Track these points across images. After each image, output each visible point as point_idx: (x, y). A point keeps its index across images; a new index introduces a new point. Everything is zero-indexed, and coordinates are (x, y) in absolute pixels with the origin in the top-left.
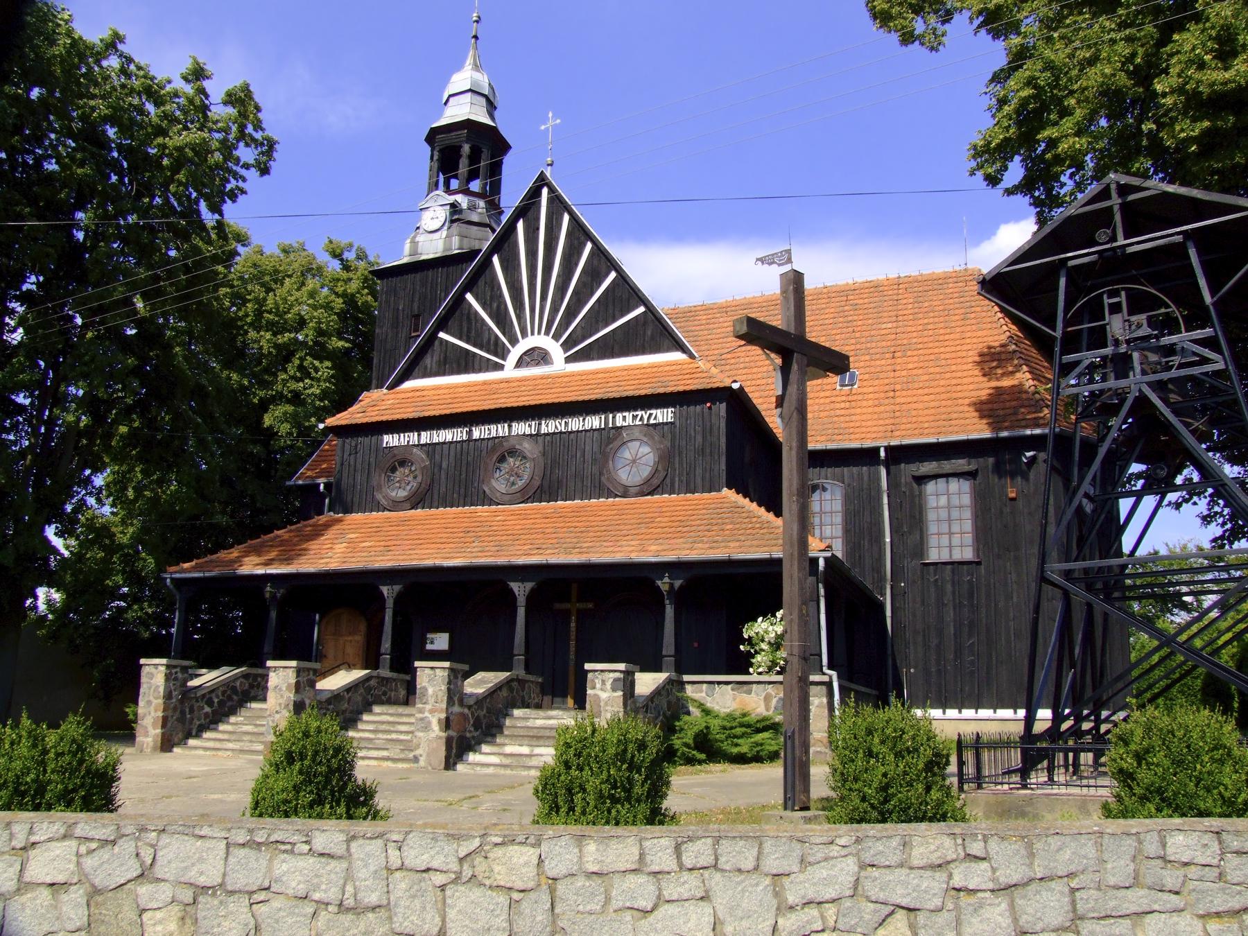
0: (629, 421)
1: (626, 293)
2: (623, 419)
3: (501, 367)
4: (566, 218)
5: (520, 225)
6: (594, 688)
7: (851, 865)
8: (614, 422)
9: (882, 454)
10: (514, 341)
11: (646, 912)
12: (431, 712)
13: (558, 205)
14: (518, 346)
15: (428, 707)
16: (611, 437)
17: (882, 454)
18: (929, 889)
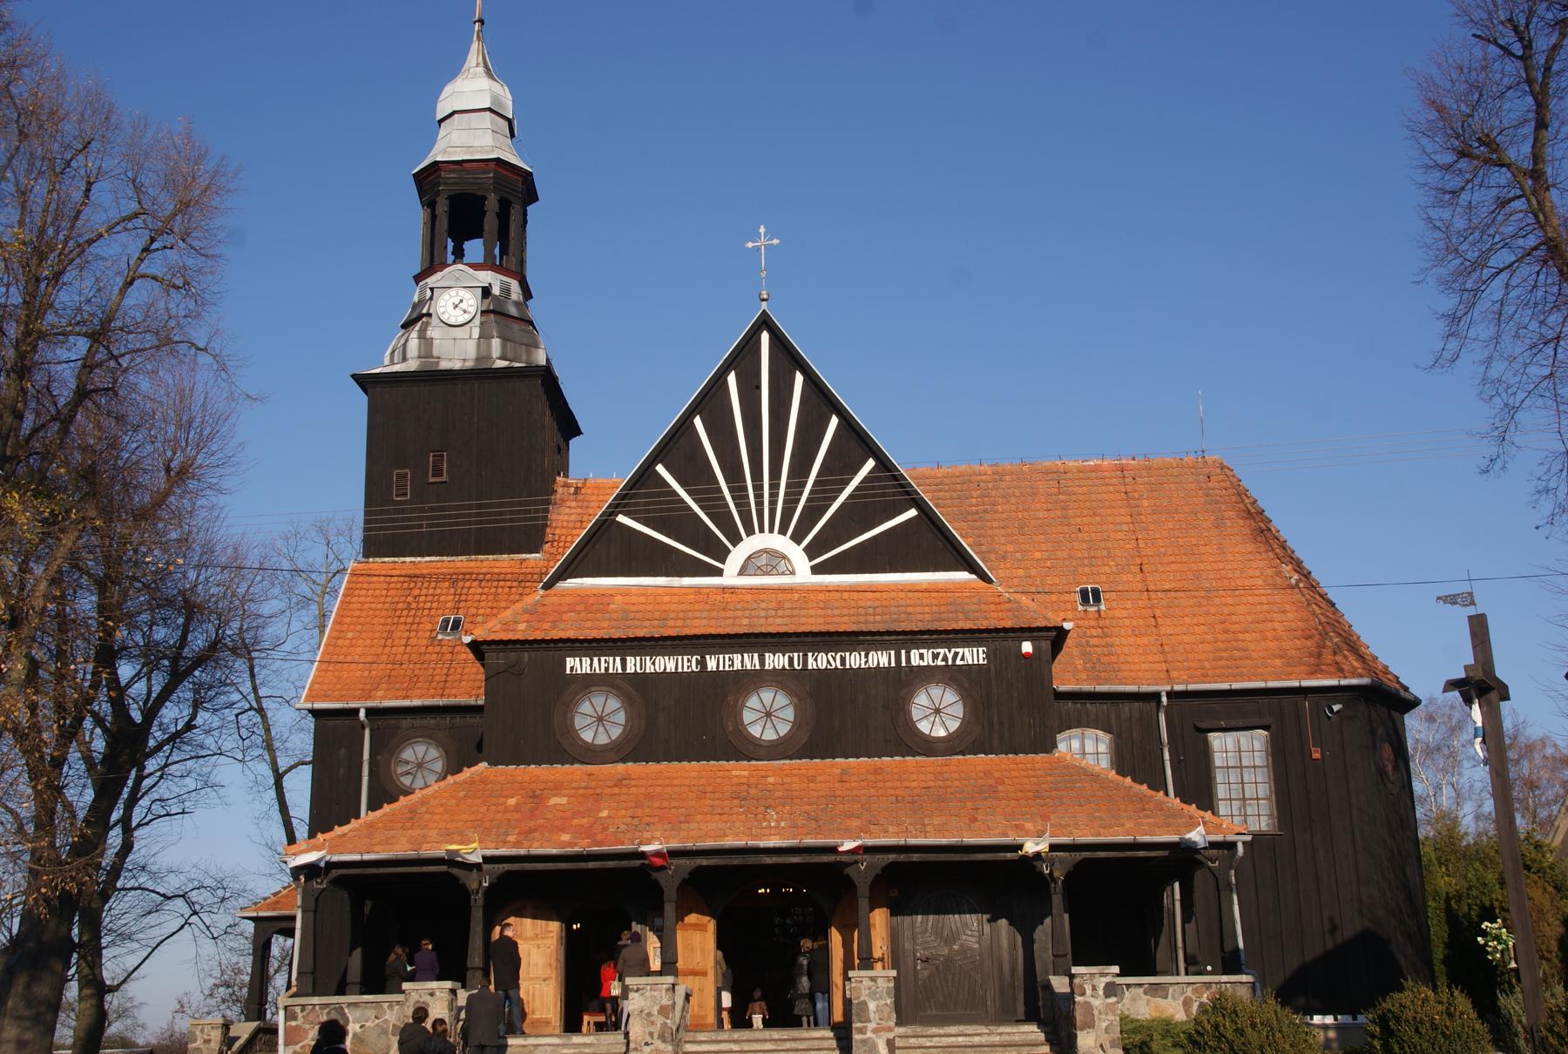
0: (928, 660)
1: (891, 488)
2: (920, 657)
3: (719, 572)
4: (799, 378)
5: (732, 379)
6: (1083, 994)
9: (1164, 699)
10: (736, 539)
12: (875, 1031)
13: (788, 358)
15: (871, 1026)
16: (905, 681)
17: (1164, 699)
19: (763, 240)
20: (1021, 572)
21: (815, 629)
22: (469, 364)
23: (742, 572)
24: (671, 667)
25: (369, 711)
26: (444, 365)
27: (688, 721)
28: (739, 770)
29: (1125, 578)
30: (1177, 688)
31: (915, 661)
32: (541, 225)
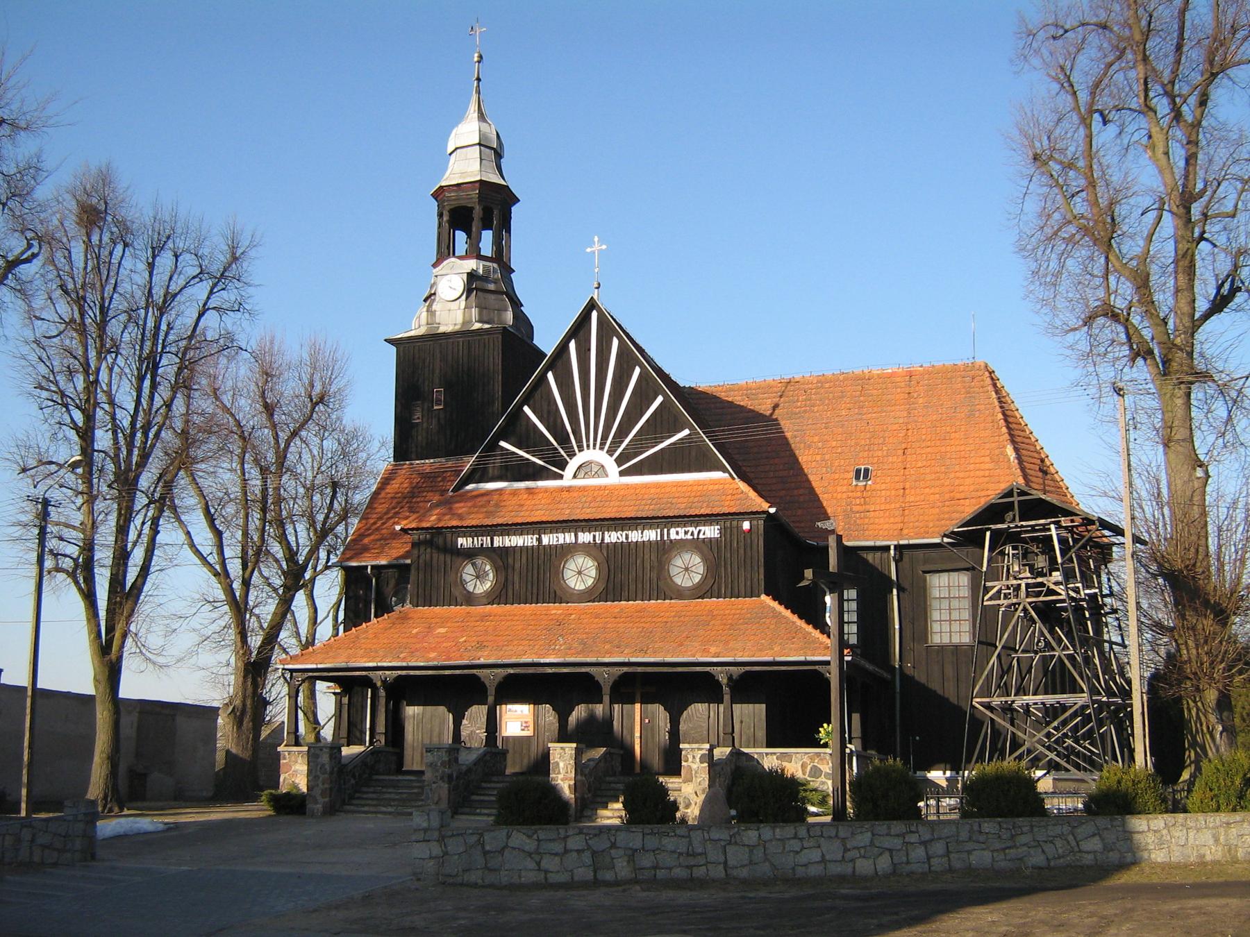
0: (682, 536)
3: (561, 477)
4: (615, 342)
7: (869, 834)
8: (668, 534)
10: (572, 455)
11: (797, 853)
13: (608, 328)
14: (575, 458)
15: (561, 776)
16: (664, 550)
18: (897, 843)
19: (597, 247)
20: (818, 458)
21: (608, 516)
22: (458, 327)
23: (575, 476)
24: (520, 543)
25: (373, 567)
26: (442, 329)
27: (529, 579)
28: (556, 609)
29: (890, 459)
30: (902, 542)
31: (673, 536)
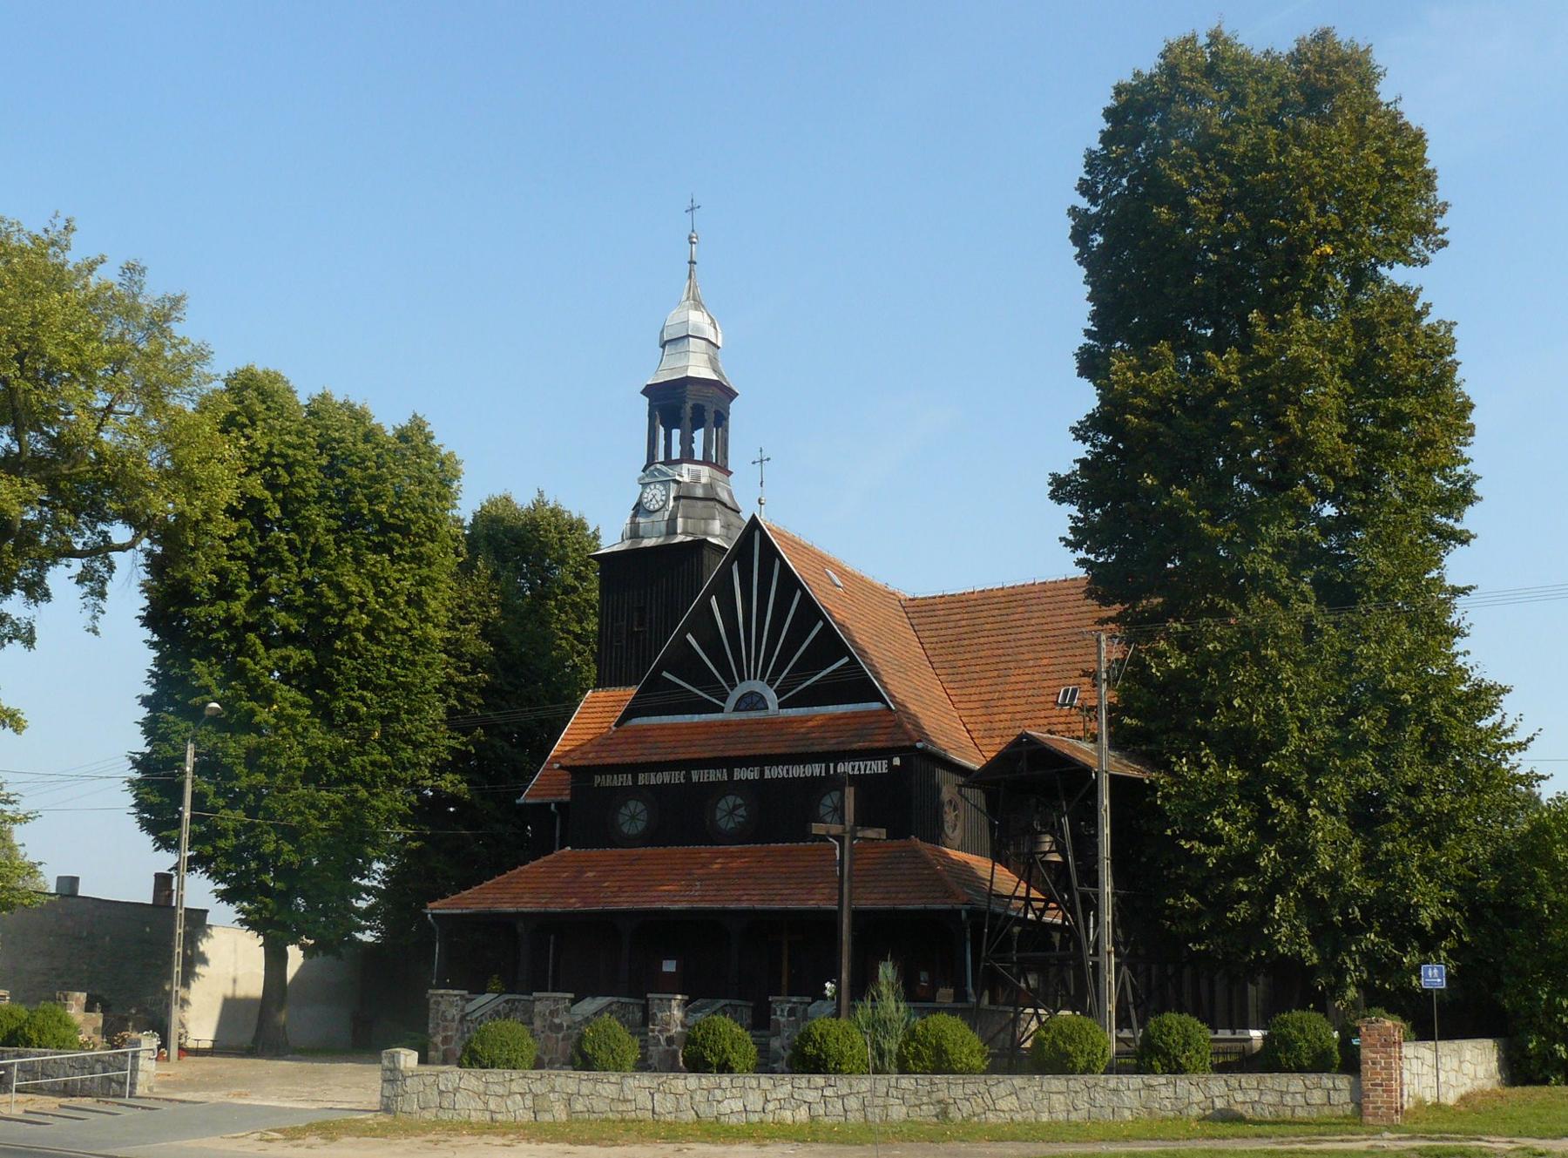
3: (721, 710)
5: (735, 567)
10: (733, 686)
23: (735, 710)
27: (682, 816)
32: (745, 425)
